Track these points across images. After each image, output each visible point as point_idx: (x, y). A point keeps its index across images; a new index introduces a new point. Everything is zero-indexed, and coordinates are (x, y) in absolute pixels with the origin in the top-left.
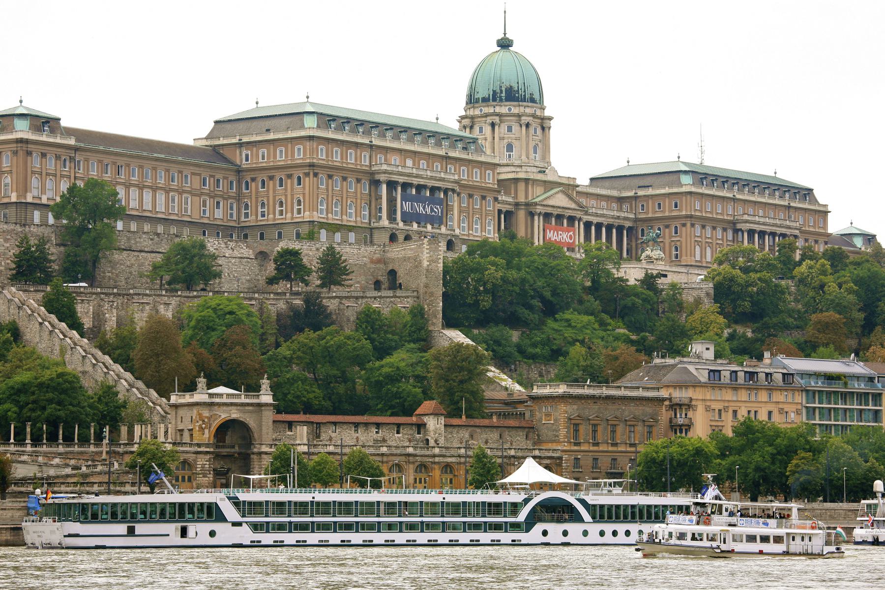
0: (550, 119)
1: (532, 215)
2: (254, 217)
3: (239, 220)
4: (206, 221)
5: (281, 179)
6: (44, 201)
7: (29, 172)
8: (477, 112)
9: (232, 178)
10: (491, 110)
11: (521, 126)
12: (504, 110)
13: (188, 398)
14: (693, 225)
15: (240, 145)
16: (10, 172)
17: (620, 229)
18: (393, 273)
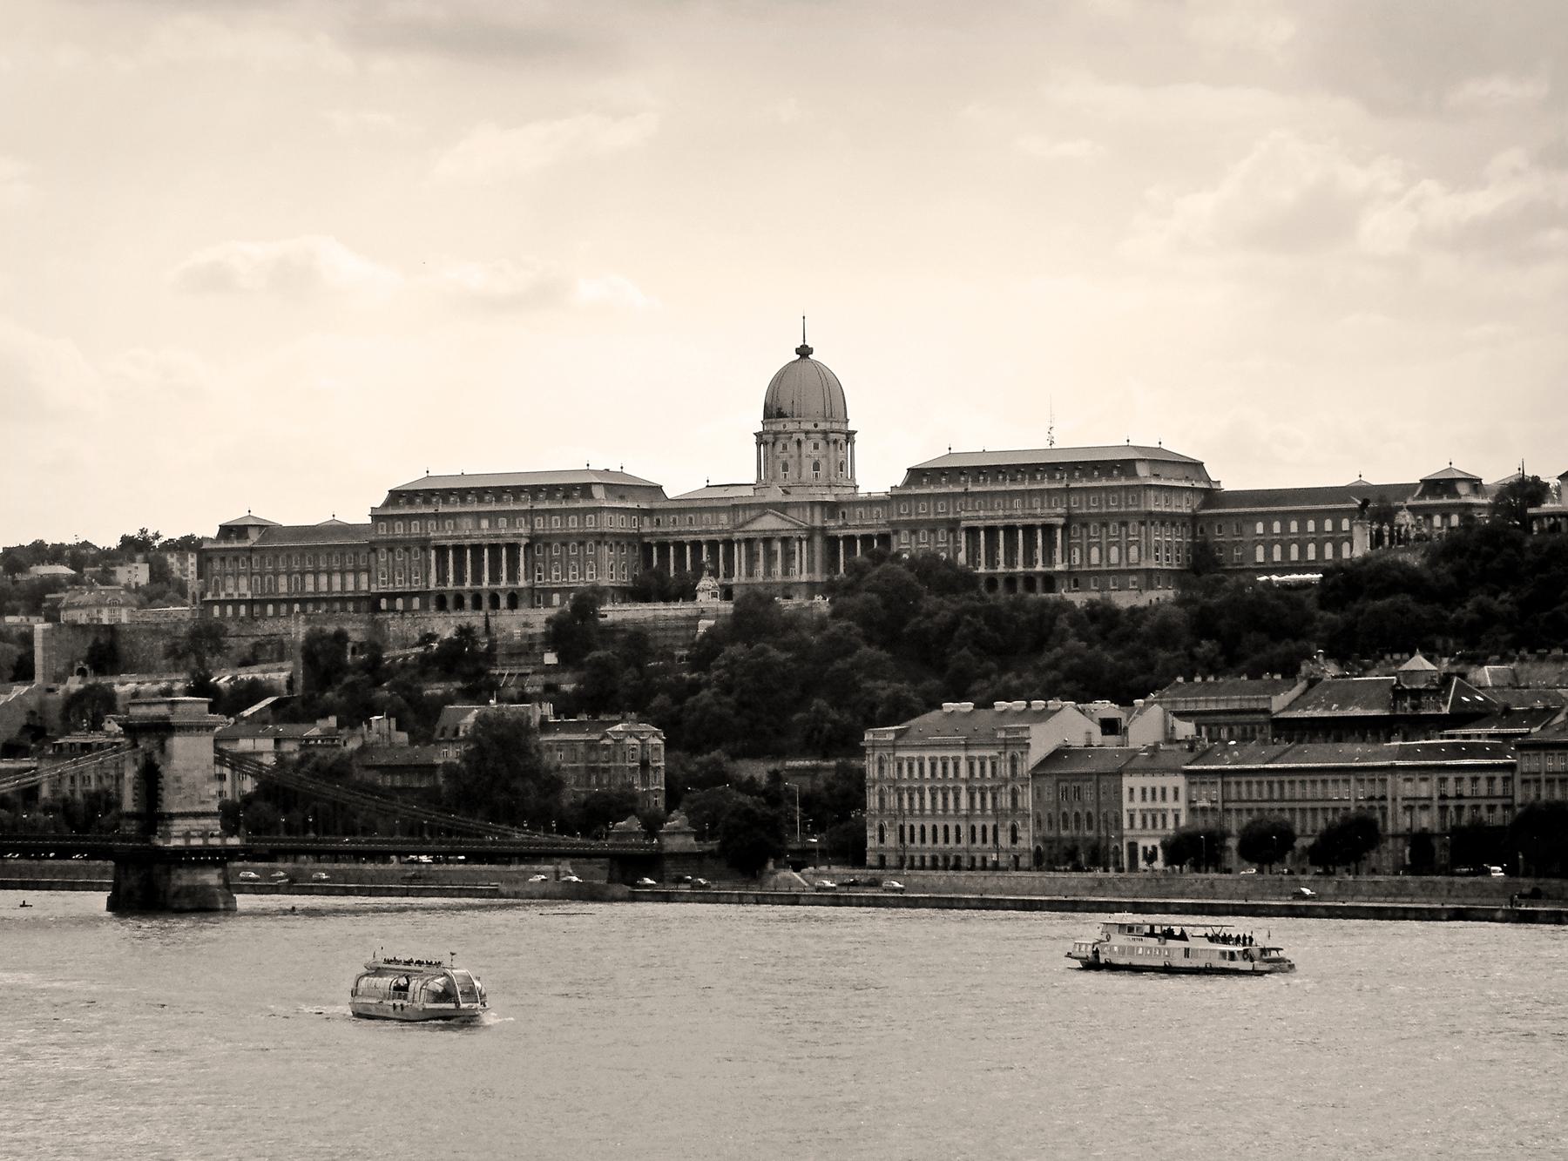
6: (222, 596)
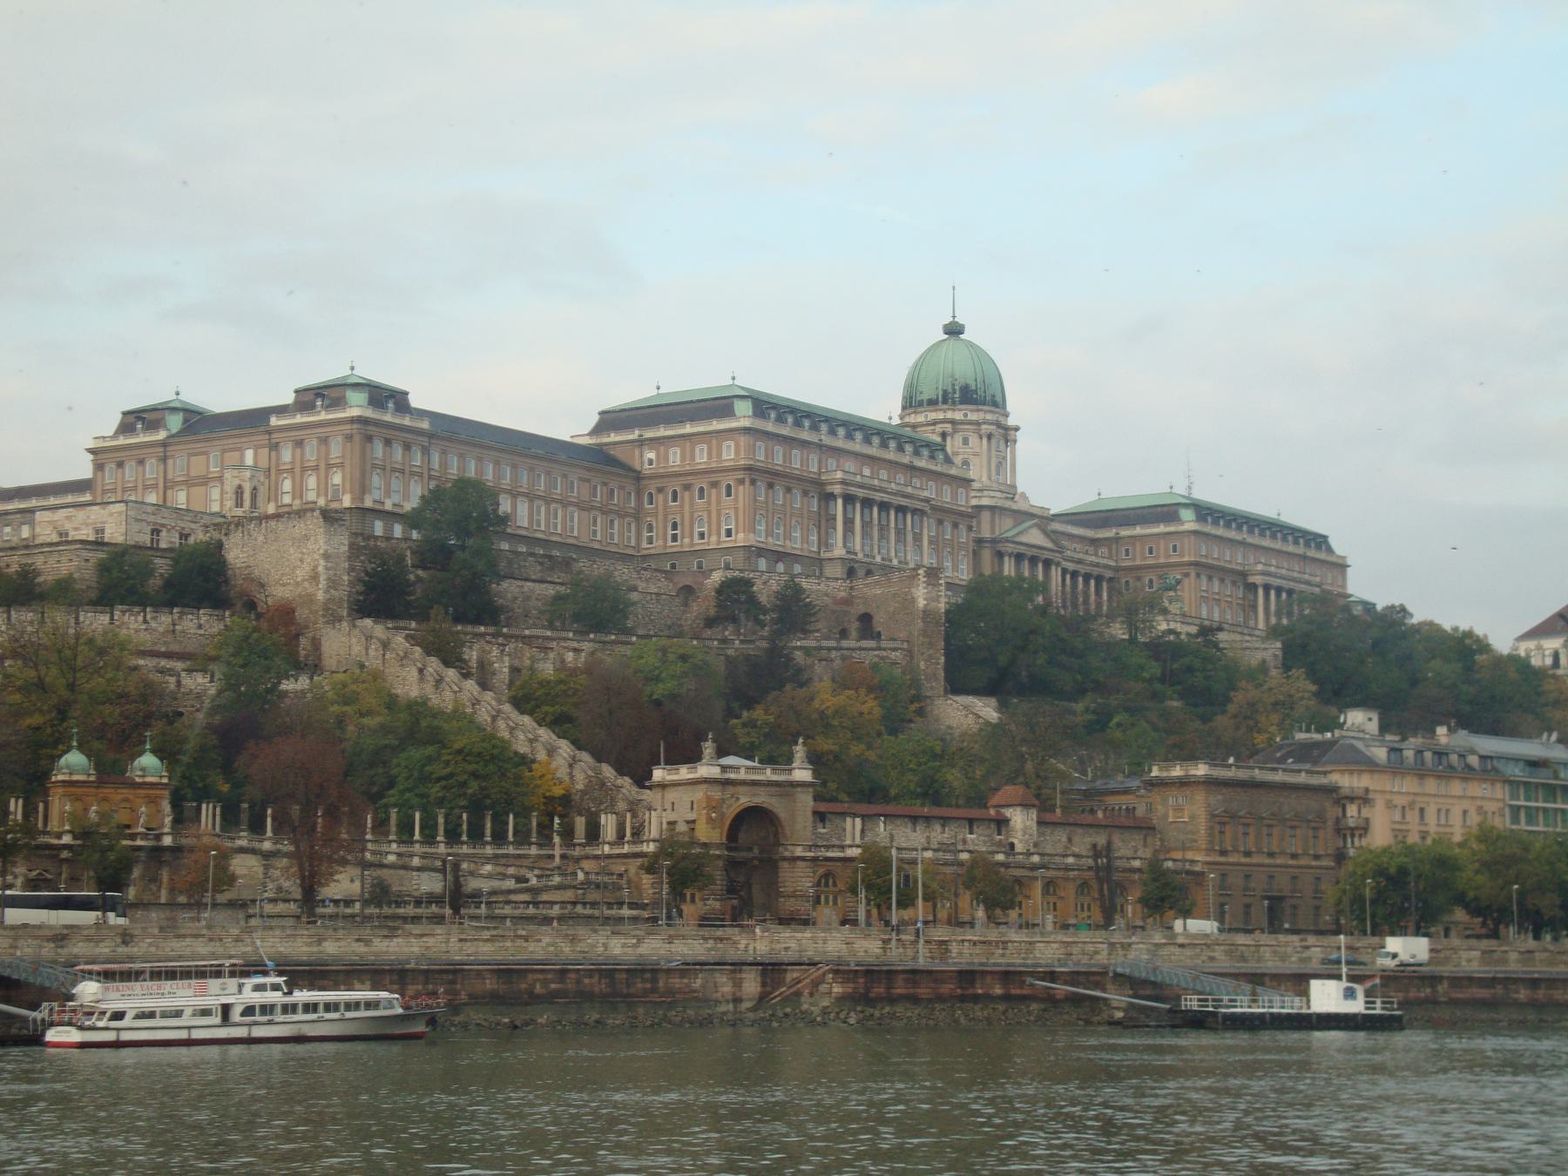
0: (1017, 429)
1: (1000, 555)
2: (661, 542)
3: (638, 547)
4: (597, 546)
5: (702, 490)
6: (388, 506)
7: (368, 467)
8: (921, 418)
9: (631, 488)
10: (941, 416)
11: (981, 437)
12: (958, 416)
13: (684, 773)
14: (1198, 575)
15: (641, 443)
16: (341, 465)
17: (1099, 579)
18: (866, 619)
